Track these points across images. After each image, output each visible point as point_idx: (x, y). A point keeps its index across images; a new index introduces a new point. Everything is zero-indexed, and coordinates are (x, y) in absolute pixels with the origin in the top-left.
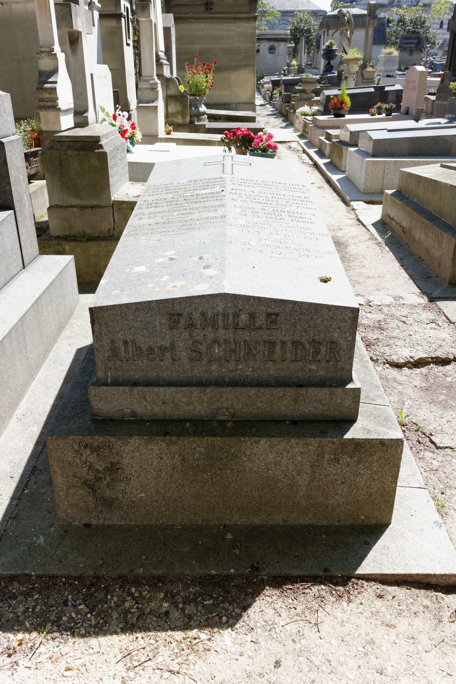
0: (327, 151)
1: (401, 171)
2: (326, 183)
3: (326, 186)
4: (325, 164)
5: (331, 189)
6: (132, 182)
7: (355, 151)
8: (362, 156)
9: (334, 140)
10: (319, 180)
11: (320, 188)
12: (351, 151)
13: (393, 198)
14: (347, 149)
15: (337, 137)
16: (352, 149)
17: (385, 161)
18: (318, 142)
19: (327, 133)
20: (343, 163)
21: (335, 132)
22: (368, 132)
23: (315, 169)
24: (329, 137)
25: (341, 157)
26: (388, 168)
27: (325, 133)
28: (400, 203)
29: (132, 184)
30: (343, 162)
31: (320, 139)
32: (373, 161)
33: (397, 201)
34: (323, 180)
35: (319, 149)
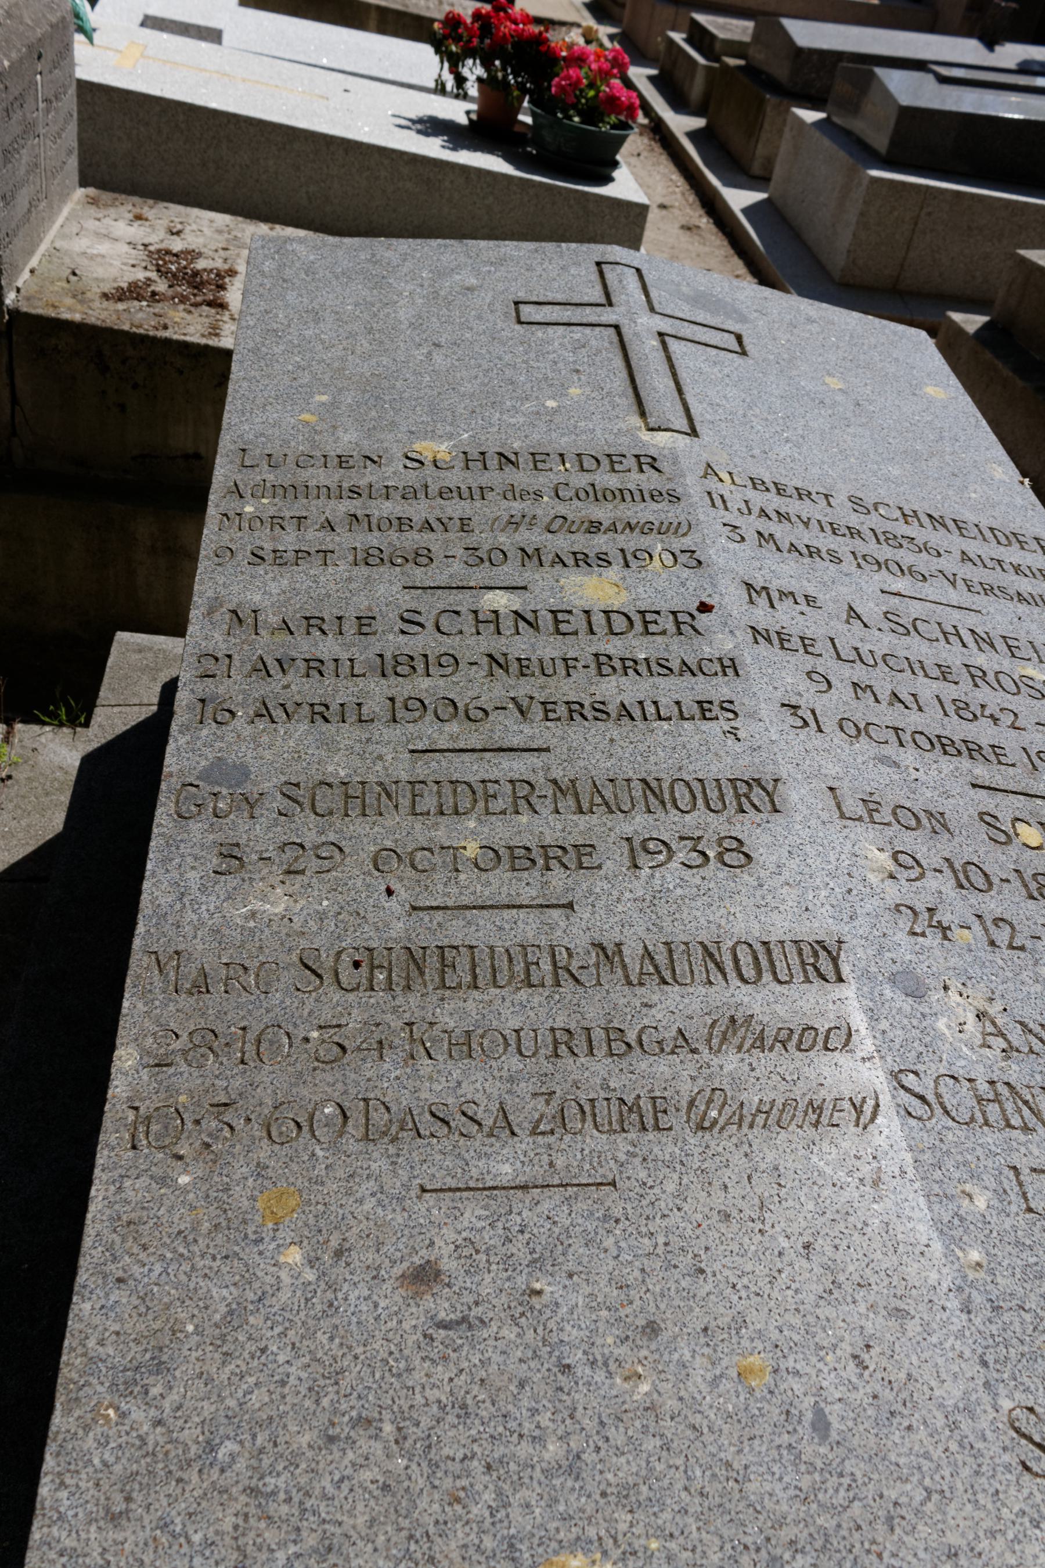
0: (697, 89)
1: (1024, 260)
2: (701, 212)
3: (705, 222)
4: (692, 135)
5: (726, 243)
6: (91, 191)
7: (818, 124)
8: (851, 155)
9: (732, 62)
10: (679, 196)
11: (689, 229)
12: (801, 122)
13: (988, 355)
14: (787, 110)
15: (735, 48)
16: (810, 116)
17: (928, 187)
18: (662, 47)
19: (695, 24)
20: (761, 151)
21: (723, 28)
22: (880, 71)
23: (657, 148)
24: (700, 37)
25: (753, 127)
26: (929, 214)
27: (686, 25)
28: (1020, 383)
29: (94, 202)
30: (760, 146)
31: (671, 42)
32: (892, 182)
33: (1006, 372)
34: (692, 198)
35: (662, 71)
